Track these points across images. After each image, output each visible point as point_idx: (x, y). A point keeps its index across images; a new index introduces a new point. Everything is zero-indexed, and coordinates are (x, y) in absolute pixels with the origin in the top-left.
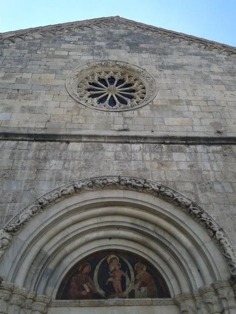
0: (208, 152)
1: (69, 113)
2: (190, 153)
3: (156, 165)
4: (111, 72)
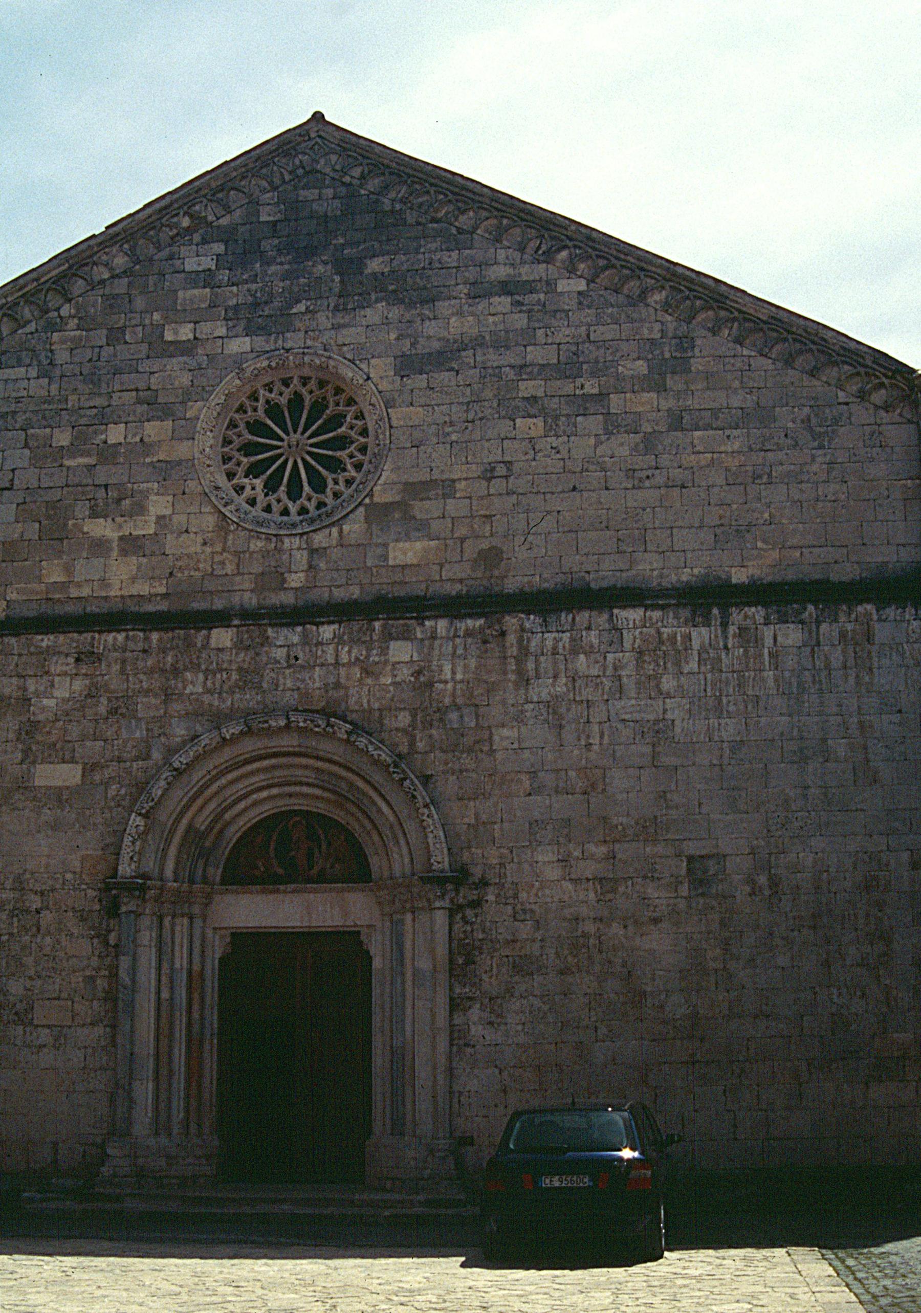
0: (456, 636)
1: (208, 550)
2: (422, 640)
3: (357, 672)
4: (295, 381)
